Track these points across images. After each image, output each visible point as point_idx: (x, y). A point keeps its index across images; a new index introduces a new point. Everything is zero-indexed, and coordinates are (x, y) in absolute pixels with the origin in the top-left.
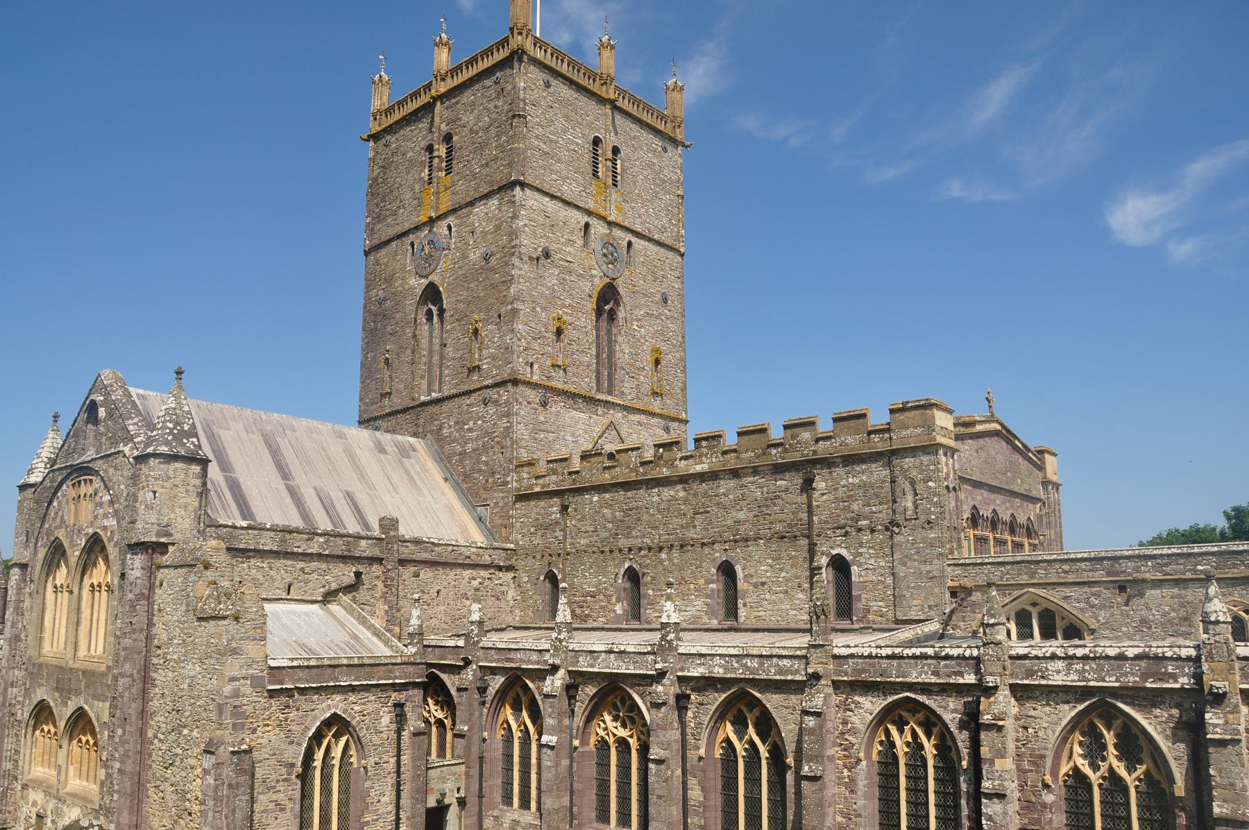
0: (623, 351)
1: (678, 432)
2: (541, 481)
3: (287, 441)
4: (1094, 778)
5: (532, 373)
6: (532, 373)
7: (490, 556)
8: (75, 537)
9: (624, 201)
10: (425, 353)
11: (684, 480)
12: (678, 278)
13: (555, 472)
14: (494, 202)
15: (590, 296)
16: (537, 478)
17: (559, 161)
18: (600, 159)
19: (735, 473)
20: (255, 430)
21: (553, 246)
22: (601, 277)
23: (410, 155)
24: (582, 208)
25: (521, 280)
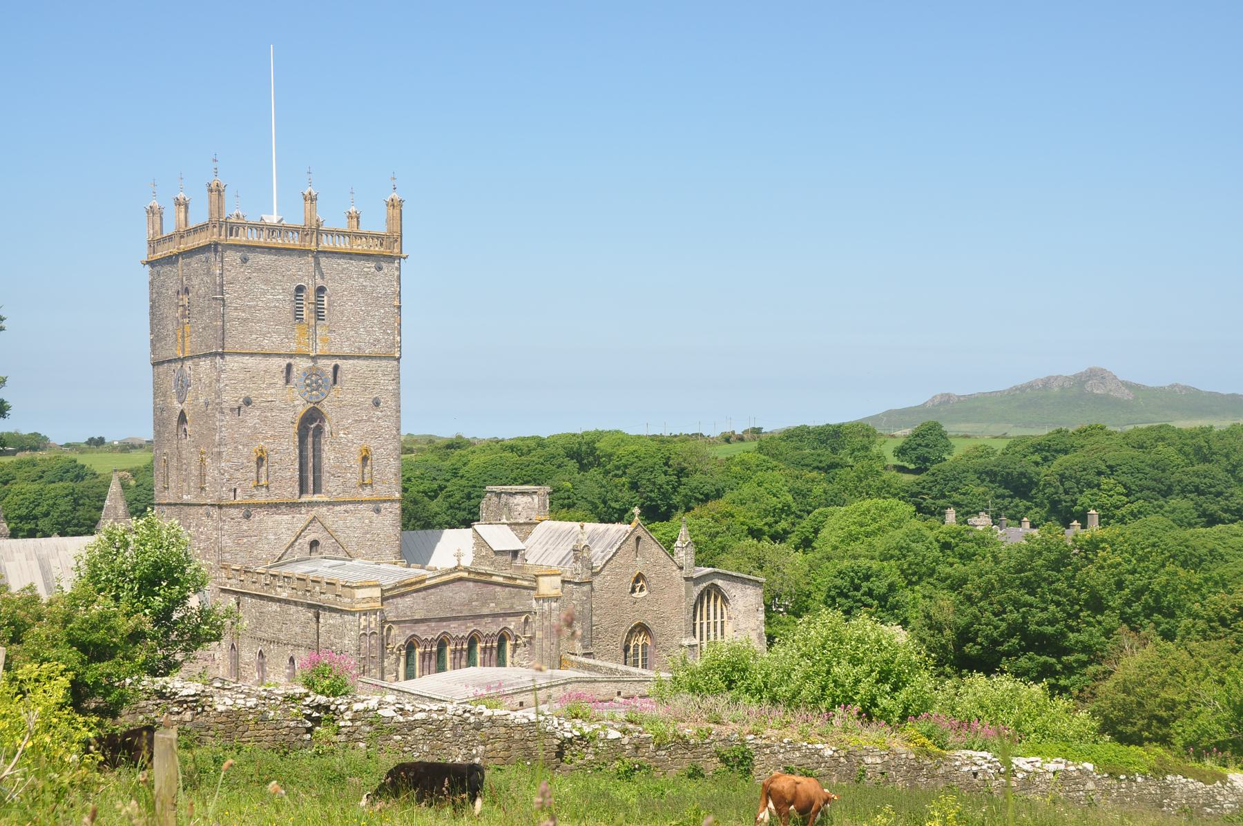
0: (329, 456)
1: (390, 510)
2: (230, 581)
3: (58, 560)
9: (330, 331)
11: (279, 600)
12: (393, 380)
15: (292, 423)
16: (229, 579)
17: (259, 321)
18: (304, 303)
19: (296, 603)
20: (34, 557)
21: (252, 395)
22: (304, 405)
25: (223, 429)
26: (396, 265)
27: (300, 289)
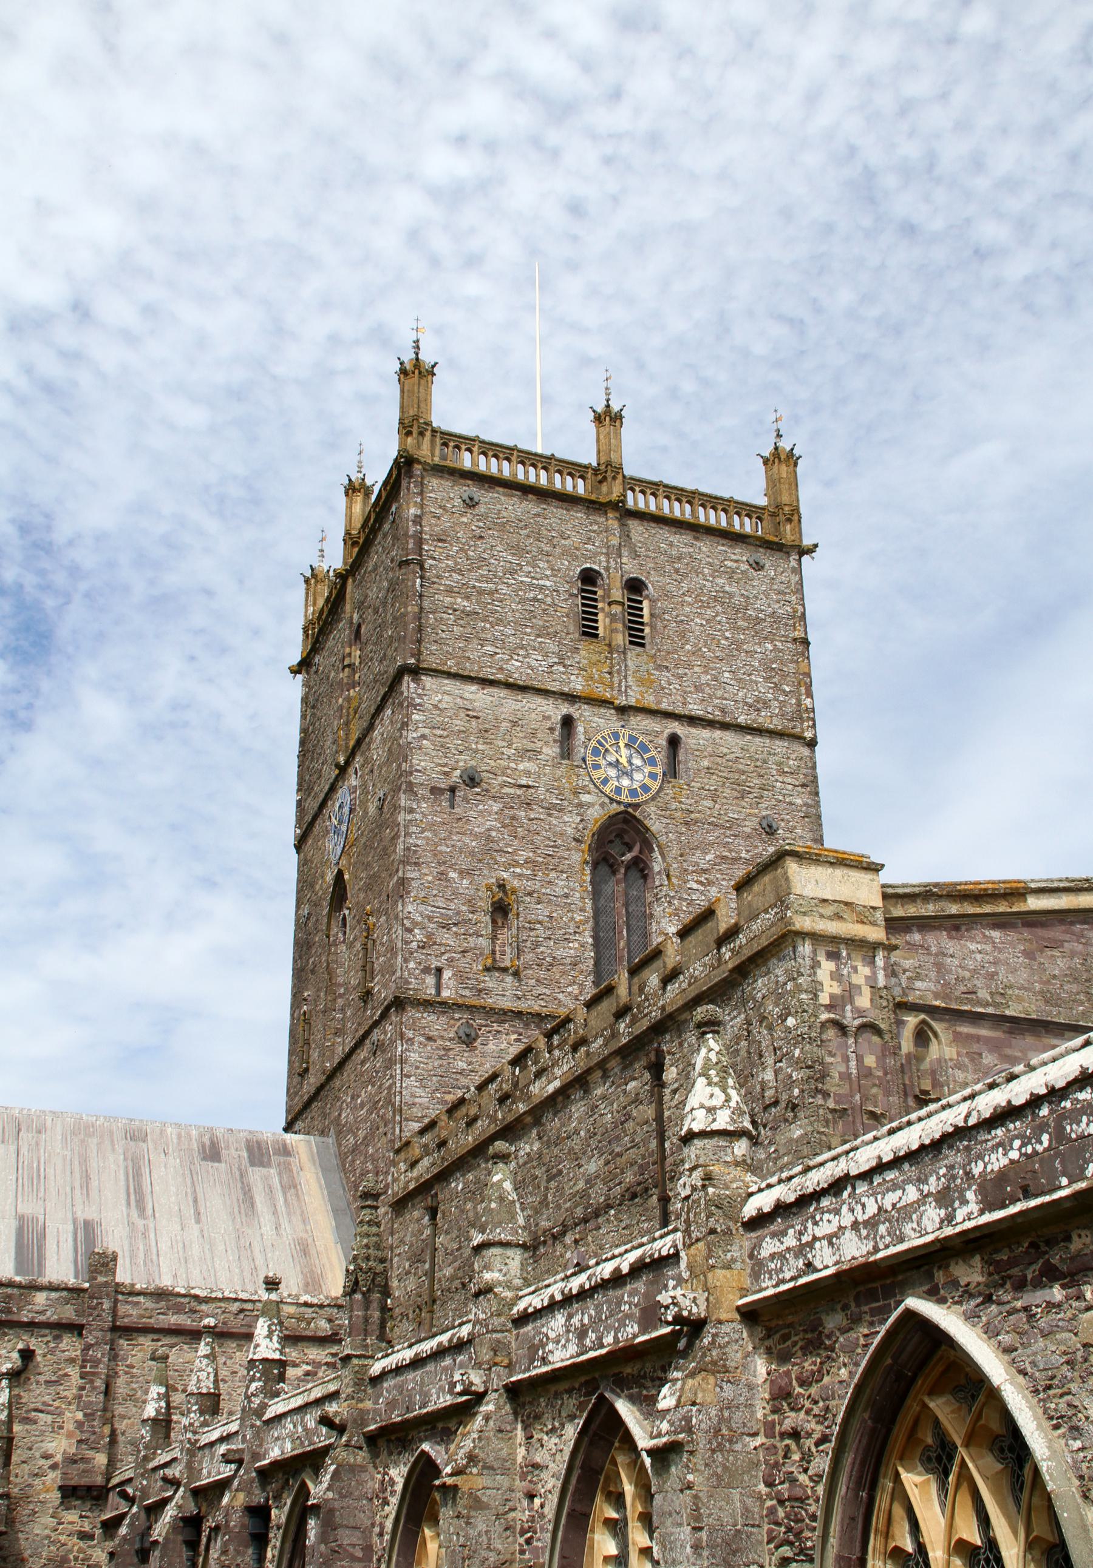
5: (438, 987)
6: (438, 987)
7: (330, 1321)
9: (659, 668)
10: (342, 991)
12: (803, 785)
15: (576, 840)
17: (499, 622)
18: (600, 605)
22: (602, 805)
24: (554, 693)
25: (414, 829)
26: (793, 564)
27: (589, 578)
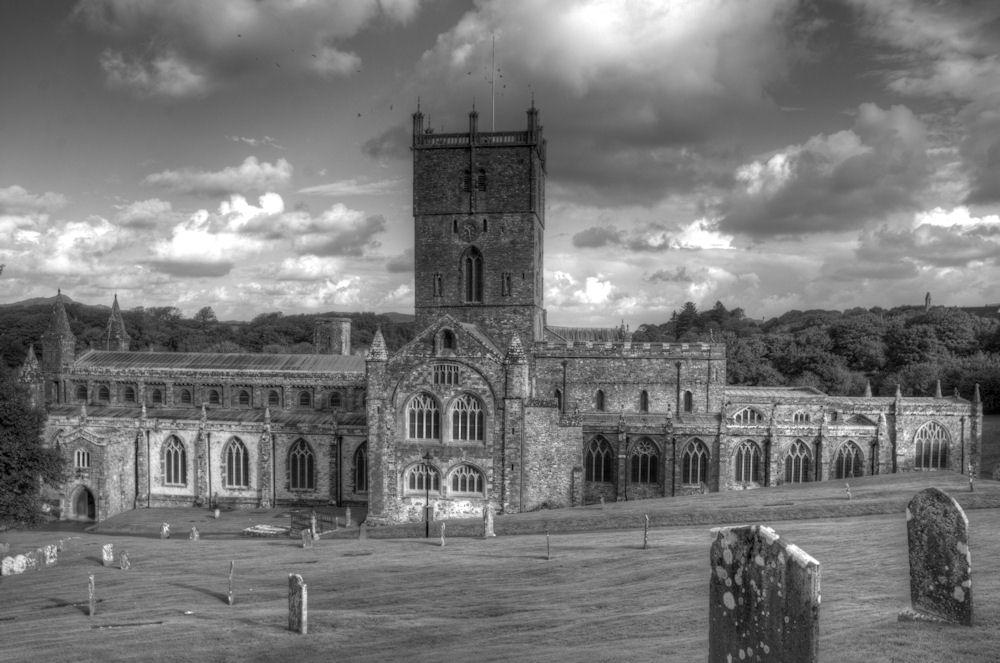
4: (793, 457)
8: (442, 390)
13: (559, 349)
14: (518, 218)
23: (450, 171)
